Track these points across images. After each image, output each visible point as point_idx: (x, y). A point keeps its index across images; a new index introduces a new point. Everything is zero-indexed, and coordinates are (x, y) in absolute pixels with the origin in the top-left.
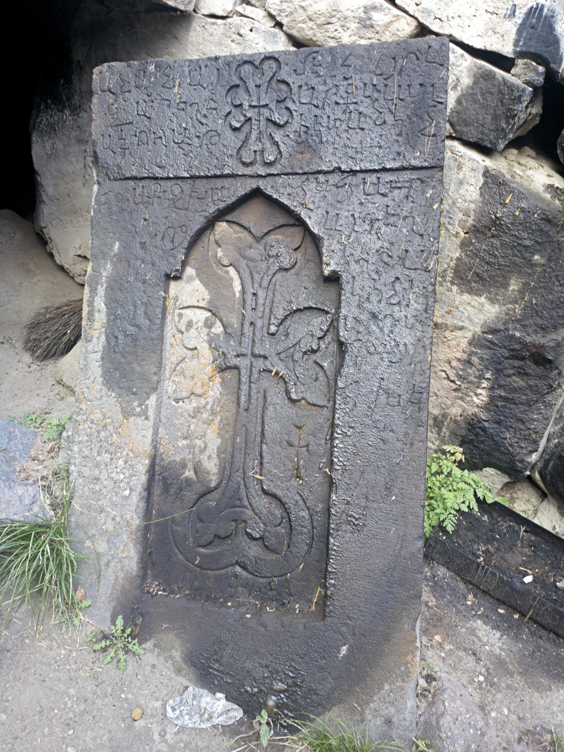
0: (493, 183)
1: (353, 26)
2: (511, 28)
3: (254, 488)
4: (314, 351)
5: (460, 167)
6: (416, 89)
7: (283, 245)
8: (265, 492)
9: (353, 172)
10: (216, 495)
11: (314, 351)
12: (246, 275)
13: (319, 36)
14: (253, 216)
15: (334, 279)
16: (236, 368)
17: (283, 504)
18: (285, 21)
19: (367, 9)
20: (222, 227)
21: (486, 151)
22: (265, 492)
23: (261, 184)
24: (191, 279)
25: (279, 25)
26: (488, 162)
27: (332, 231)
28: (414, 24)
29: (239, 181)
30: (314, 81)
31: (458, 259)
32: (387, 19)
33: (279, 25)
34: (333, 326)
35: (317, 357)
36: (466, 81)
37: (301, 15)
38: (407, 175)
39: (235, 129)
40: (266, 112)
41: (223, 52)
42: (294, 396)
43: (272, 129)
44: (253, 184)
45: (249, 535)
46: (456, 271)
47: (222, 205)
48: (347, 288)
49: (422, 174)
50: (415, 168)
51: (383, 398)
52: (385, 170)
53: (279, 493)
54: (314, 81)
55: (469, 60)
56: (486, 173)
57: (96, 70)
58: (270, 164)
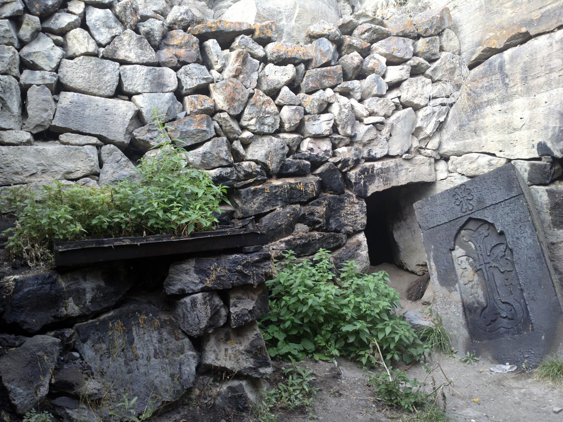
0: (550, 193)
1: (487, 167)
2: (535, 150)
3: (499, 302)
4: (504, 256)
5: (538, 192)
6: (506, 178)
7: (484, 230)
8: (504, 303)
9: (497, 204)
10: (487, 309)
11: (504, 256)
12: (475, 242)
13: (477, 173)
14: (471, 225)
15: (502, 233)
16: (481, 269)
17: (509, 304)
18: (464, 173)
19: (489, 161)
20: (463, 232)
21: (545, 185)
22: (504, 303)
23: (471, 216)
24: (458, 249)
25: (463, 175)
26: (547, 188)
27: (496, 221)
28: (505, 160)
29: (464, 218)
30: (477, 186)
31: (552, 219)
32: (496, 161)
33: (463, 175)
34: (507, 246)
35: (506, 257)
36: (528, 168)
37: (469, 170)
38: (513, 199)
39: (458, 205)
40: (466, 198)
41: (448, 188)
42: (502, 271)
43: (469, 201)
44: (468, 217)
45: (501, 317)
46: (553, 223)
47: (461, 225)
48: (506, 234)
49: (517, 197)
50: (514, 197)
51: (529, 260)
52: (506, 200)
53: (507, 301)
54: (477, 186)
55: (527, 163)
56: (547, 191)
57: (414, 205)
58: (472, 210)
